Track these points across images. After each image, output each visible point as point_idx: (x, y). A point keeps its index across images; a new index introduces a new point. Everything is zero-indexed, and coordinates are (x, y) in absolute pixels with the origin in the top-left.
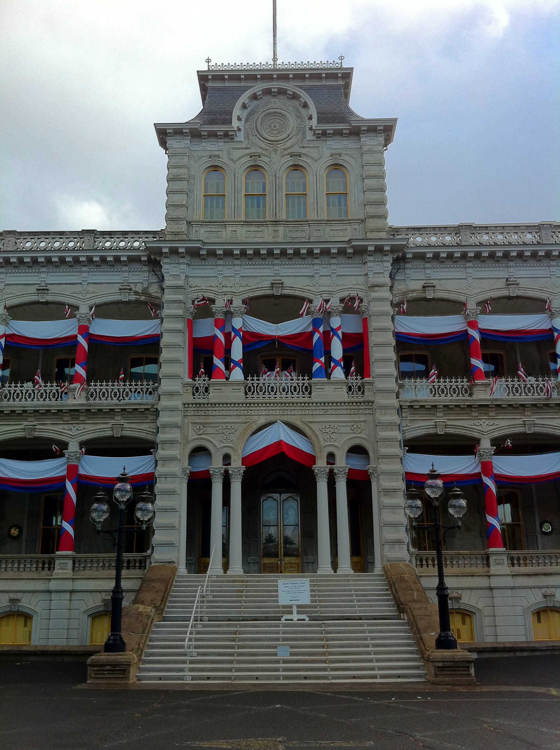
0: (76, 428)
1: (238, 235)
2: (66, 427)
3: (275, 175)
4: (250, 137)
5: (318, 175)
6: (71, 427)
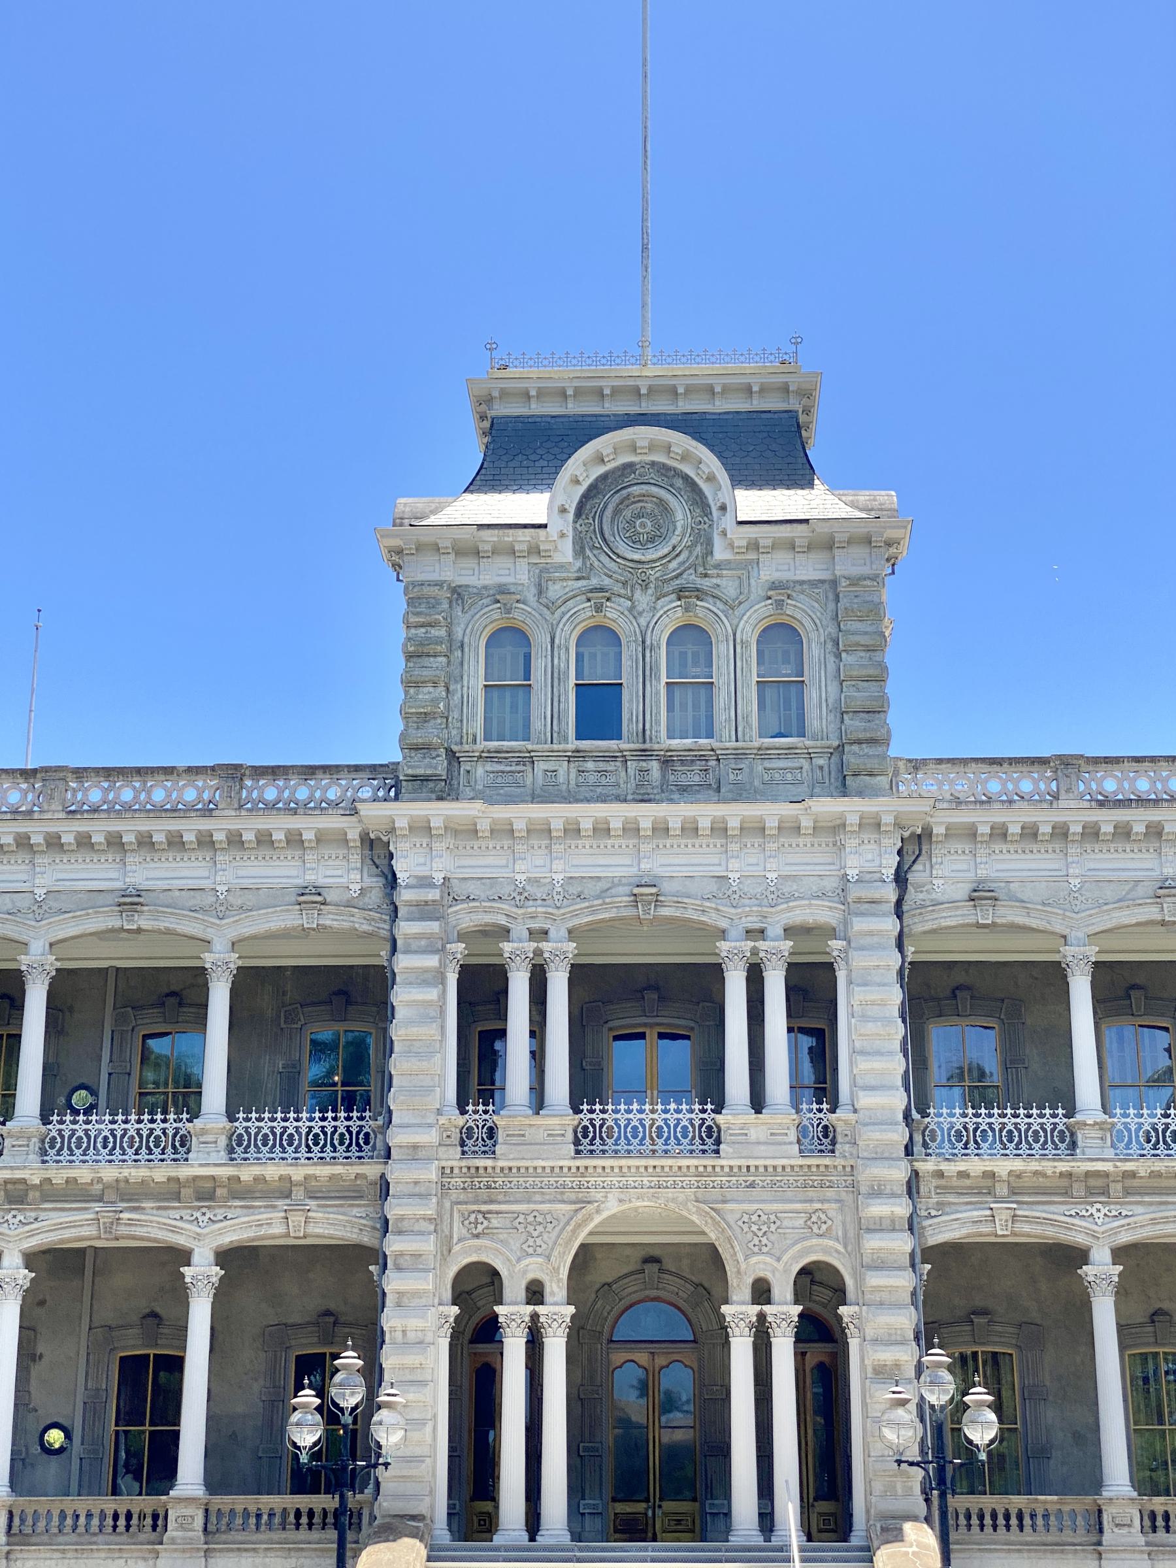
0: (208, 1216)
1: (561, 779)
2: (186, 1213)
3: (644, 642)
4: (588, 552)
5: (738, 640)
6: (197, 1214)
